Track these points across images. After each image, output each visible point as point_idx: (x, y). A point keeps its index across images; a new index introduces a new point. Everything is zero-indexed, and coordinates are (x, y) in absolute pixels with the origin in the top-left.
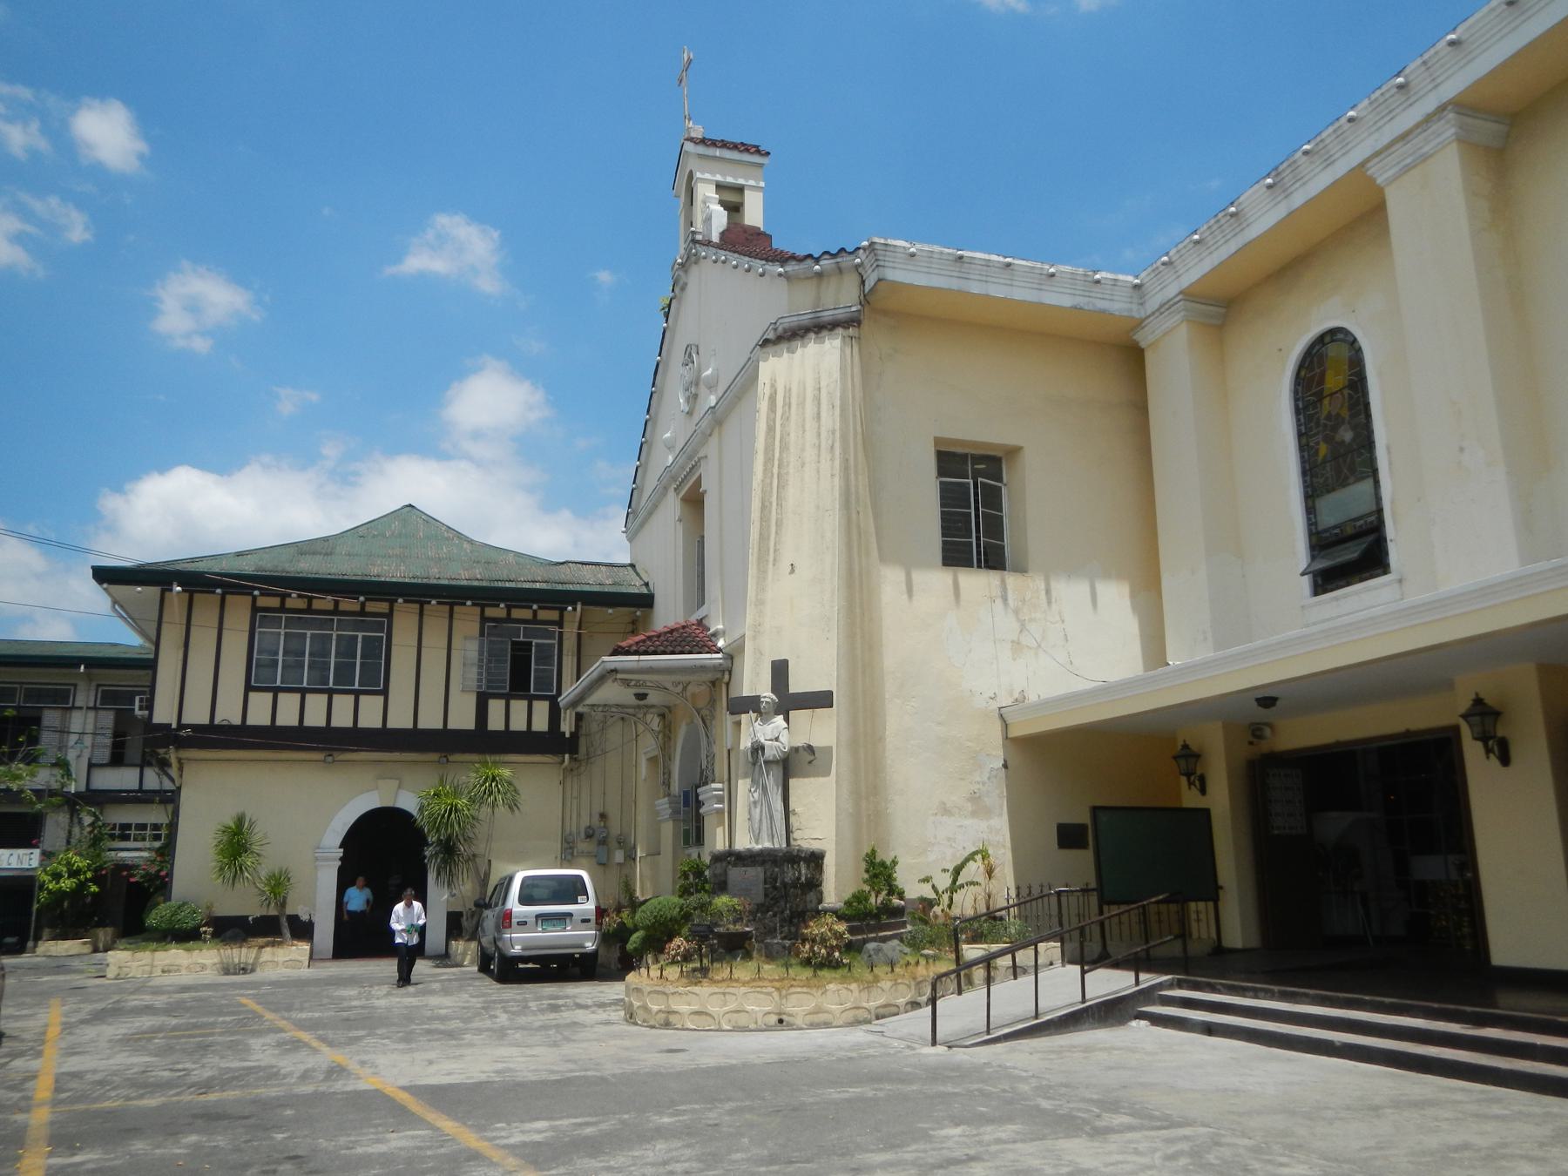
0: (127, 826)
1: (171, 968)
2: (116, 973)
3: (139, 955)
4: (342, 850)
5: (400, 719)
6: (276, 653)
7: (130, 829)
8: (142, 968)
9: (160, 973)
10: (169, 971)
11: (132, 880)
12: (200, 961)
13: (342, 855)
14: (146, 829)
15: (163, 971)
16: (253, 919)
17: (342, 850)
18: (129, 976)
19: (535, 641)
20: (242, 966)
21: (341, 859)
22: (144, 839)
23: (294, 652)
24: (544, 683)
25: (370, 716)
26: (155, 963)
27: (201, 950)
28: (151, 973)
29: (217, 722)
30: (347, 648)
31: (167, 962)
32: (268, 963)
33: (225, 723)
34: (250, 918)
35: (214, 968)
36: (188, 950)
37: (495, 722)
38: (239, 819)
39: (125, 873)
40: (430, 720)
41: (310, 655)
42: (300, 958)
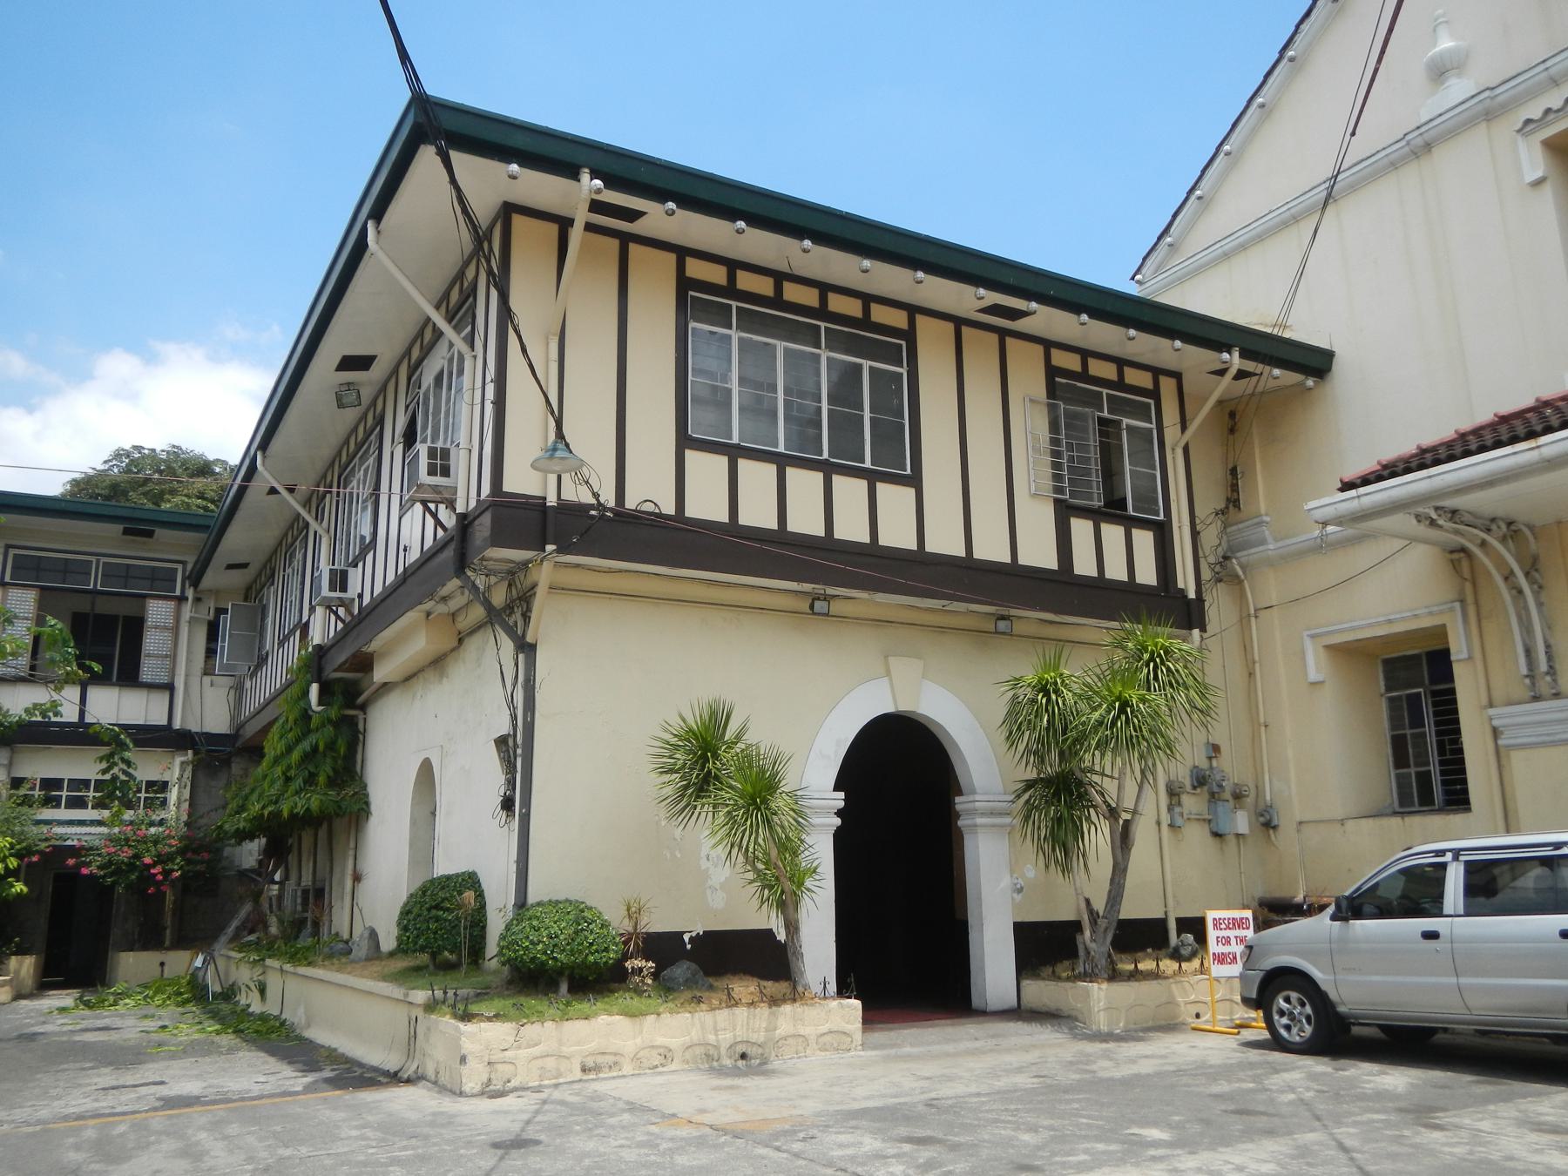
0: (55, 784)
1: (600, 1059)
2: (485, 1078)
3: (532, 1030)
4: (842, 795)
5: (945, 540)
6: (726, 377)
7: (61, 789)
8: (539, 1062)
9: (578, 1075)
10: (597, 1068)
11: (85, 871)
12: (660, 1041)
13: (842, 804)
14: (61, 789)
15: (584, 1070)
16: (691, 939)
17: (842, 795)
18: (511, 1085)
19: (1126, 421)
20: (741, 1049)
21: (839, 813)
22: (58, 806)
23: (758, 386)
24: (1146, 499)
25: (897, 534)
26: (566, 1050)
27: (659, 1014)
28: (559, 1075)
29: (630, 504)
30: (846, 383)
31: (592, 1046)
32: (790, 1041)
33: (649, 507)
34: (686, 938)
35: (688, 1055)
36: (630, 1014)
37: (1084, 565)
38: (713, 714)
39: (71, 862)
40: (991, 548)
41: (787, 391)
42: (848, 1028)
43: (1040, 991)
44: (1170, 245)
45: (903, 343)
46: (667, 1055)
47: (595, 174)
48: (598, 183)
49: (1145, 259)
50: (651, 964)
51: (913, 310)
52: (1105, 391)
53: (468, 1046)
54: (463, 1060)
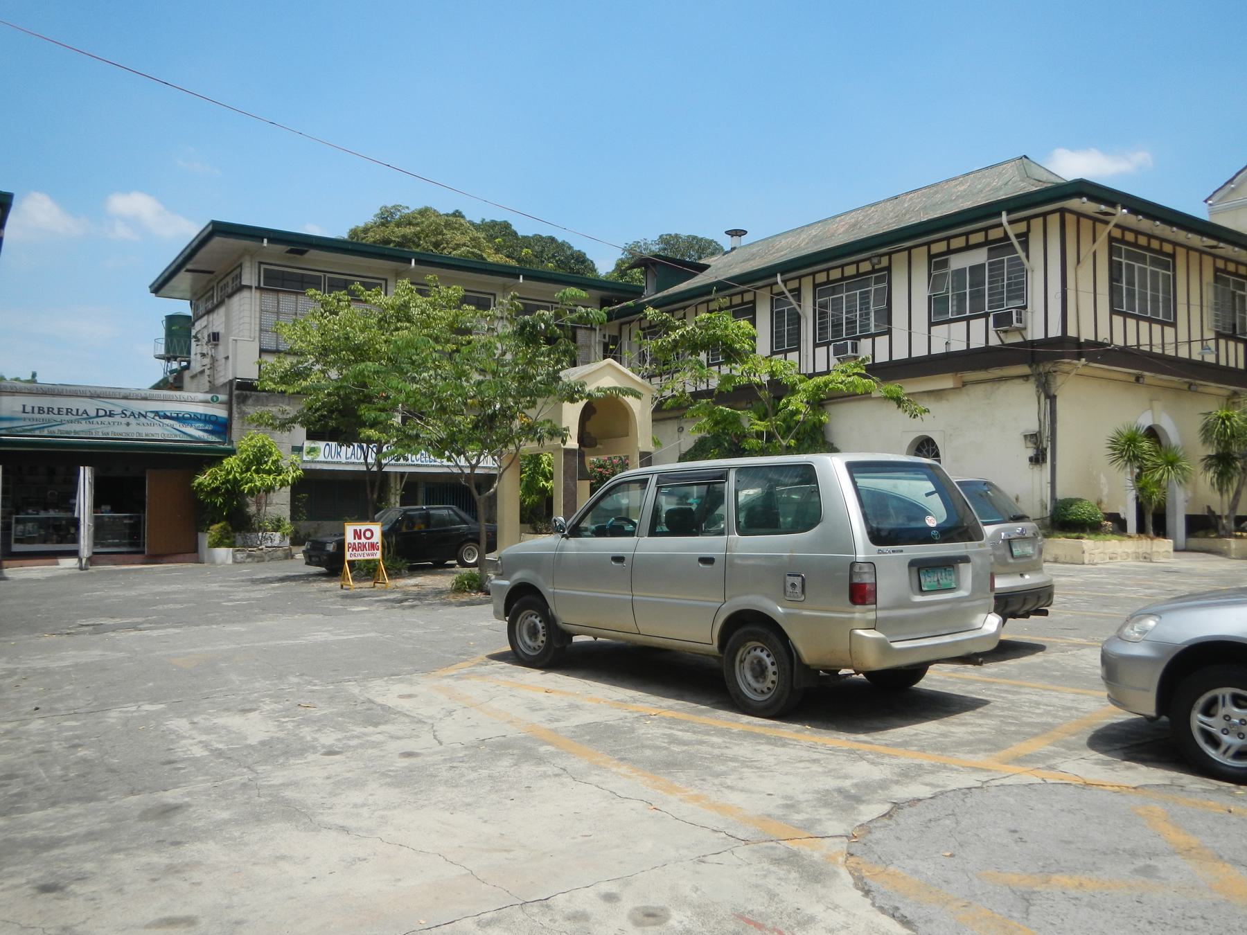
9: (1108, 560)
12: (1126, 550)
15: (1110, 559)
36: (1119, 541)
43: (1194, 542)
44: (1233, 189)
45: (1171, 260)
46: (1128, 554)
47: (1123, 207)
48: (1125, 211)
49: (1215, 192)
50: (1110, 523)
51: (1175, 244)
52: (1231, 278)
53: (1085, 548)
54: (1084, 552)
